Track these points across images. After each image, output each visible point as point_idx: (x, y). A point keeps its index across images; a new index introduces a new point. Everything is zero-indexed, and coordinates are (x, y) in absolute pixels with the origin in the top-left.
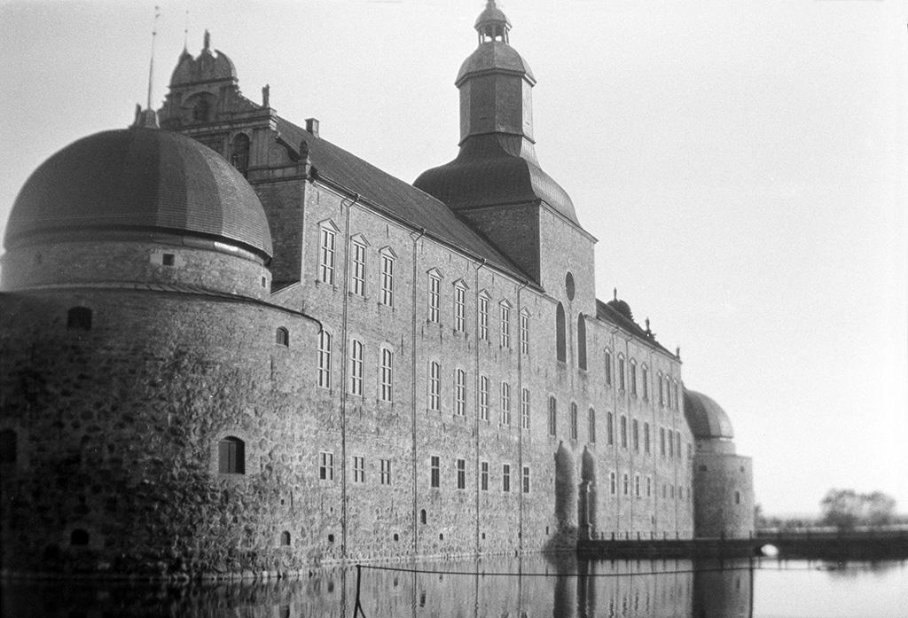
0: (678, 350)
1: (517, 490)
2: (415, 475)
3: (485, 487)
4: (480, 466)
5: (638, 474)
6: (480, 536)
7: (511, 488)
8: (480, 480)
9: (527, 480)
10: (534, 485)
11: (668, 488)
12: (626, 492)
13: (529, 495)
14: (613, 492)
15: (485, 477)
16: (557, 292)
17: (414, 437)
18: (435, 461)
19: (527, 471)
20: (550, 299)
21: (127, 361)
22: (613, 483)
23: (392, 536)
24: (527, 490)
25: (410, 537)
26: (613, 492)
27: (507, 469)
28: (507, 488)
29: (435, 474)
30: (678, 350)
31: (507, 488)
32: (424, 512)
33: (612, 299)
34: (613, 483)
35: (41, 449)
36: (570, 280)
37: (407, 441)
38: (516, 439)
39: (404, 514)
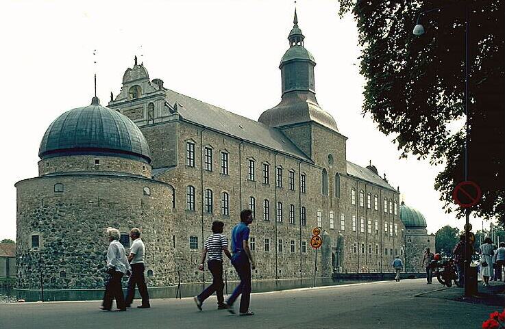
1: (299, 251)
3: (281, 250)
7: (295, 251)
13: (307, 253)
14: (355, 251)
15: (280, 246)
19: (304, 243)
26: (355, 251)
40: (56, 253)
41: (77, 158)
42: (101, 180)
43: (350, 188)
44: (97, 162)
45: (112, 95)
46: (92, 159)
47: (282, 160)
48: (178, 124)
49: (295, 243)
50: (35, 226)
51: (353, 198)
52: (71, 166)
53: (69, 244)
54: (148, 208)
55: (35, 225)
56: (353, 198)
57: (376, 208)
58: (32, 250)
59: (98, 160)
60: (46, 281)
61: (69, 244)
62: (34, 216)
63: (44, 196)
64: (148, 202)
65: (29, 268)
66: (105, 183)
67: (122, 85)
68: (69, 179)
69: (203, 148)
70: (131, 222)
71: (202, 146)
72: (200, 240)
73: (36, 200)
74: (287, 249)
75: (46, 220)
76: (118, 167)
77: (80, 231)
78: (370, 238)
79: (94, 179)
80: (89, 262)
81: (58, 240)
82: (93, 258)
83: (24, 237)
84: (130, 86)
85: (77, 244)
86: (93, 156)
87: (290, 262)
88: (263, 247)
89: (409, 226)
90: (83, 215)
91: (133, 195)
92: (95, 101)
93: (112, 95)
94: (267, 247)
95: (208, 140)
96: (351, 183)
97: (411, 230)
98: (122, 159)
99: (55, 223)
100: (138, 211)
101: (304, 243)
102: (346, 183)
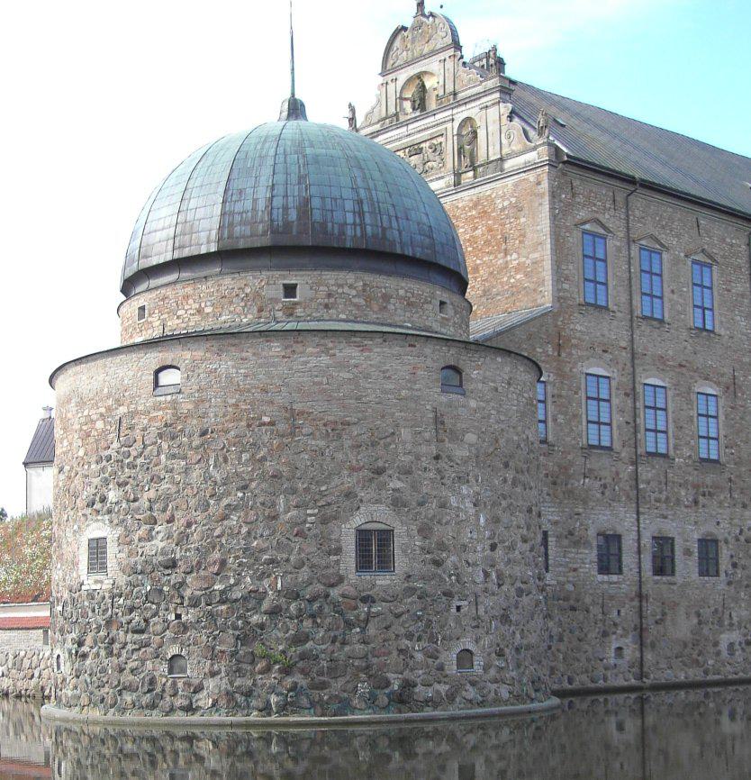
35: (130, 554)
42: (299, 348)
44: (290, 290)
45: (352, 110)
50: (98, 506)
52: (208, 310)
54: (456, 437)
55: (97, 503)
58: (90, 583)
60: (129, 688)
63: (123, 410)
65: (80, 644)
67: (381, 80)
69: (635, 250)
70: (399, 485)
71: (630, 241)
72: (628, 543)
73: (100, 425)
81: (163, 552)
86: (277, 274)
91: (404, 393)
93: (352, 110)
95: (649, 214)
98: (369, 278)
100: (424, 449)
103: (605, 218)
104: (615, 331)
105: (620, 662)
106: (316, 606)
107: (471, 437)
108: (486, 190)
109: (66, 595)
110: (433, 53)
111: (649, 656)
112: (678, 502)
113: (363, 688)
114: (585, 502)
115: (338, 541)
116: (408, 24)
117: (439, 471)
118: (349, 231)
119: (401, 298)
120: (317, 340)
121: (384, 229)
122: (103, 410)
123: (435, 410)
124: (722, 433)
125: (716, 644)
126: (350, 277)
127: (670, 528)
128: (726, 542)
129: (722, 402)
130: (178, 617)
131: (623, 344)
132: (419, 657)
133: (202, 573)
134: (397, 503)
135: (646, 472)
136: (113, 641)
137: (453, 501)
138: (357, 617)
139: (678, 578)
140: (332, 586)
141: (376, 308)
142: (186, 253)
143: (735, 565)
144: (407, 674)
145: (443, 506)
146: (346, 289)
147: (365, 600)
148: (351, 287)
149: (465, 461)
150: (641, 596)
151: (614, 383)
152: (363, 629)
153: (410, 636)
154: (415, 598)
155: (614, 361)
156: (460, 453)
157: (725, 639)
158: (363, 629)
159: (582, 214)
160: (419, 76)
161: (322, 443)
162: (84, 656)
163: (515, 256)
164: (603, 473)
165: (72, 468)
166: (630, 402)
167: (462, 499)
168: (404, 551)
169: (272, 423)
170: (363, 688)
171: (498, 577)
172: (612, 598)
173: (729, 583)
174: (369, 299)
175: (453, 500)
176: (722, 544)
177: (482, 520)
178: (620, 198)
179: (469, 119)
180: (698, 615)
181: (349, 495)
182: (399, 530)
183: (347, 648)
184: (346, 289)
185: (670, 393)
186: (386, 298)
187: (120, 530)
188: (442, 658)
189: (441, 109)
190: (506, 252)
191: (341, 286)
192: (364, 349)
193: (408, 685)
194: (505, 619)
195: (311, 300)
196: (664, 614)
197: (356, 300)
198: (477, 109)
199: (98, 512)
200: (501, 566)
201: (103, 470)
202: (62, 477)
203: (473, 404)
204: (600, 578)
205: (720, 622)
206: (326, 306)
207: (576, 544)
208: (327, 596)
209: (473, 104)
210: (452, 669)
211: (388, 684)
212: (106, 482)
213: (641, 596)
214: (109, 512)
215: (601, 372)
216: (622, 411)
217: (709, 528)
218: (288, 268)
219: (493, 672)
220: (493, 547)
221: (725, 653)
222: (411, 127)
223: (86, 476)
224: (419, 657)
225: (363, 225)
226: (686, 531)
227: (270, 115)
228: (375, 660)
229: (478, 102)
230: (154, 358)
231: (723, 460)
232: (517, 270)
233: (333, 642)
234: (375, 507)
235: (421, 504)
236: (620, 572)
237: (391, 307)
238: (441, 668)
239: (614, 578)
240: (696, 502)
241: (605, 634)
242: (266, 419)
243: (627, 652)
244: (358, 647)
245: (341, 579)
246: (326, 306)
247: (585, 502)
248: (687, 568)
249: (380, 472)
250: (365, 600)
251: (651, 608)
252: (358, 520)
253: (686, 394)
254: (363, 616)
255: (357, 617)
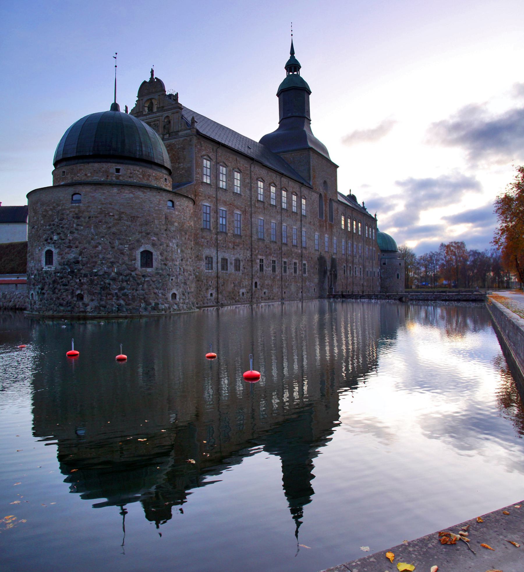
0: (375, 215)
1: (301, 273)
2: (252, 267)
4: (283, 263)
5: (355, 266)
6: (283, 292)
7: (298, 272)
8: (283, 269)
9: (305, 269)
10: (308, 271)
11: (369, 272)
12: (350, 274)
13: (306, 275)
14: (344, 273)
15: (285, 268)
16: (319, 189)
17: (251, 251)
18: (261, 260)
20: (317, 193)
21: (96, 217)
22: (344, 270)
23: (241, 293)
24: (305, 273)
25: (249, 294)
26: (344, 273)
27: (295, 264)
28: (295, 272)
29: (261, 267)
30: (375, 215)
31: (295, 272)
32: (256, 283)
33: (349, 194)
34: (344, 270)
35: (62, 258)
36: (325, 182)
37: (248, 252)
38: (300, 251)
39: (247, 283)
40: (72, 272)
41: (96, 165)
42: (123, 190)
43: (340, 213)
44: (118, 170)
45: (126, 107)
46: (112, 167)
47: (287, 183)
48: (195, 138)
49: (298, 264)
50: (49, 241)
51: (343, 222)
52: (89, 175)
53: (87, 263)
54: (172, 224)
55: (49, 240)
56: (343, 222)
57: (360, 233)
58: (46, 268)
59: (119, 169)
60: (61, 305)
61: (87, 263)
62: (49, 230)
63: (60, 208)
64: (172, 217)
65: (42, 289)
66: (127, 194)
68: (88, 189)
70: (155, 238)
72: (215, 260)
73: (50, 213)
74: (290, 271)
75: (62, 235)
76: (140, 178)
77: (100, 248)
78: (356, 260)
79: (115, 190)
80: (109, 284)
81: (74, 258)
82: (114, 279)
83: (36, 254)
84: (145, 99)
85: (96, 262)
86: (114, 164)
87: (293, 284)
88: (270, 269)
89: (383, 251)
90: (103, 229)
91: (156, 208)
92: (115, 107)
93: (126, 107)
94: (274, 270)
96: (341, 208)
97: (386, 254)
98: (144, 169)
99: (71, 238)
101: (305, 264)
102: (337, 209)
103: (210, 155)
104: (211, 191)
105: (211, 298)
106: (128, 277)
107: (176, 224)
108: (173, 141)
109: (36, 272)
110: (156, 92)
111: (220, 296)
112: (229, 248)
113: (143, 305)
114: (202, 246)
115: (135, 256)
116: (148, 80)
117: (167, 235)
118: (138, 153)
119: (154, 176)
120: (129, 188)
121: (149, 153)
122: (52, 207)
123: (165, 215)
124: (242, 226)
125: (239, 293)
126: (138, 168)
127: (226, 256)
128: (242, 261)
129: (242, 216)
130: (80, 280)
131: (214, 196)
132: (160, 295)
133: (88, 265)
134: (154, 245)
135: (220, 238)
136: (55, 289)
137: (171, 244)
138: (141, 282)
139: (229, 272)
140: (132, 271)
141: (146, 179)
142: (81, 154)
143: (244, 268)
144: (156, 301)
145: (167, 246)
146: (136, 172)
147: (143, 276)
148: (138, 171)
149: (174, 231)
150: (218, 277)
151: (211, 208)
152: (143, 286)
153: (157, 288)
154: (159, 276)
155: (211, 201)
156: (173, 229)
157: (242, 291)
158: (143, 286)
159: (204, 153)
160: (151, 99)
161: (129, 223)
162: (44, 294)
163: (182, 164)
164: (208, 237)
165: (38, 227)
166: (215, 215)
167: (173, 244)
168: (156, 260)
169: (113, 216)
170: (143, 305)
171: (184, 270)
172: (210, 277)
173: (243, 274)
174: (143, 176)
175: (171, 244)
176: (241, 262)
177: (179, 251)
178: (215, 148)
179: (168, 117)
180: (234, 283)
181: (138, 241)
182: (154, 253)
183: (138, 292)
184: (136, 172)
185: (227, 213)
186: (149, 176)
187: (57, 250)
188: (167, 296)
189: (158, 111)
190: (179, 163)
191: (135, 171)
192: (144, 193)
193: (157, 304)
194: (185, 283)
195: (125, 174)
196: (224, 283)
197: (140, 176)
198: (170, 114)
199: (49, 243)
200: (184, 266)
201: (51, 228)
202: (34, 230)
203: (177, 213)
204: (206, 271)
205: (240, 285)
206: (130, 177)
207: (199, 260)
208: (131, 274)
209: (169, 112)
210: (170, 298)
211: (151, 304)
212: (53, 233)
213: (218, 277)
214: (54, 243)
215: (208, 204)
216: (213, 218)
217: (237, 256)
218: (118, 163)
219: (181, 300)
220: (182, 260)
221: (241, 295)
222: (147, 116)
223: (44, 230)
224: (160, 295)
225: (142, 151)
226: (231, 257)
227: (107, 108)
228: (146, 296)
229: (171, 111)
230: (71, 190)
231: (242, 234)
232: (183, 169)
233: (133, 290)
234: (147, 246)
235: (161, 245)
236: (212, 269)
237: (150, 179)
238: (166, 299)
239: (210, 271)
240: (234, 248)
241: (207, 289)
242: (111, 214)
243: (214, 295)
244: (141, 291)
245: (136, 269)
246: (130, 177)
247: (202, 246)
248: (231, 268)
249: (148, 234)
250: (143, 276)
251: (221, 281)
252: (142, 249)
253: (232, 213)
254: (143, 281)
255: (141, 282)
